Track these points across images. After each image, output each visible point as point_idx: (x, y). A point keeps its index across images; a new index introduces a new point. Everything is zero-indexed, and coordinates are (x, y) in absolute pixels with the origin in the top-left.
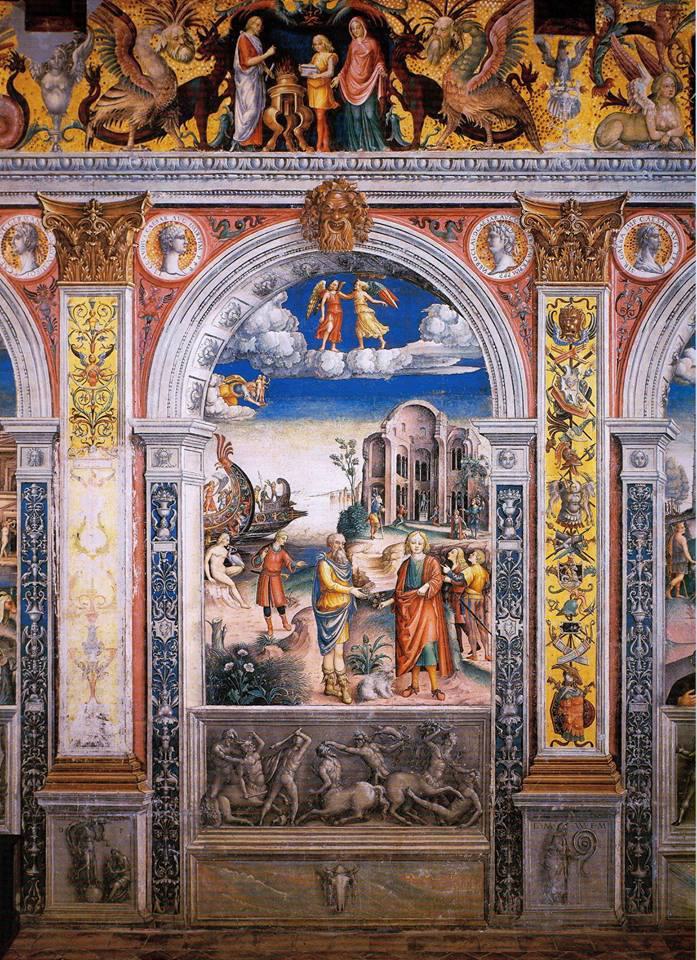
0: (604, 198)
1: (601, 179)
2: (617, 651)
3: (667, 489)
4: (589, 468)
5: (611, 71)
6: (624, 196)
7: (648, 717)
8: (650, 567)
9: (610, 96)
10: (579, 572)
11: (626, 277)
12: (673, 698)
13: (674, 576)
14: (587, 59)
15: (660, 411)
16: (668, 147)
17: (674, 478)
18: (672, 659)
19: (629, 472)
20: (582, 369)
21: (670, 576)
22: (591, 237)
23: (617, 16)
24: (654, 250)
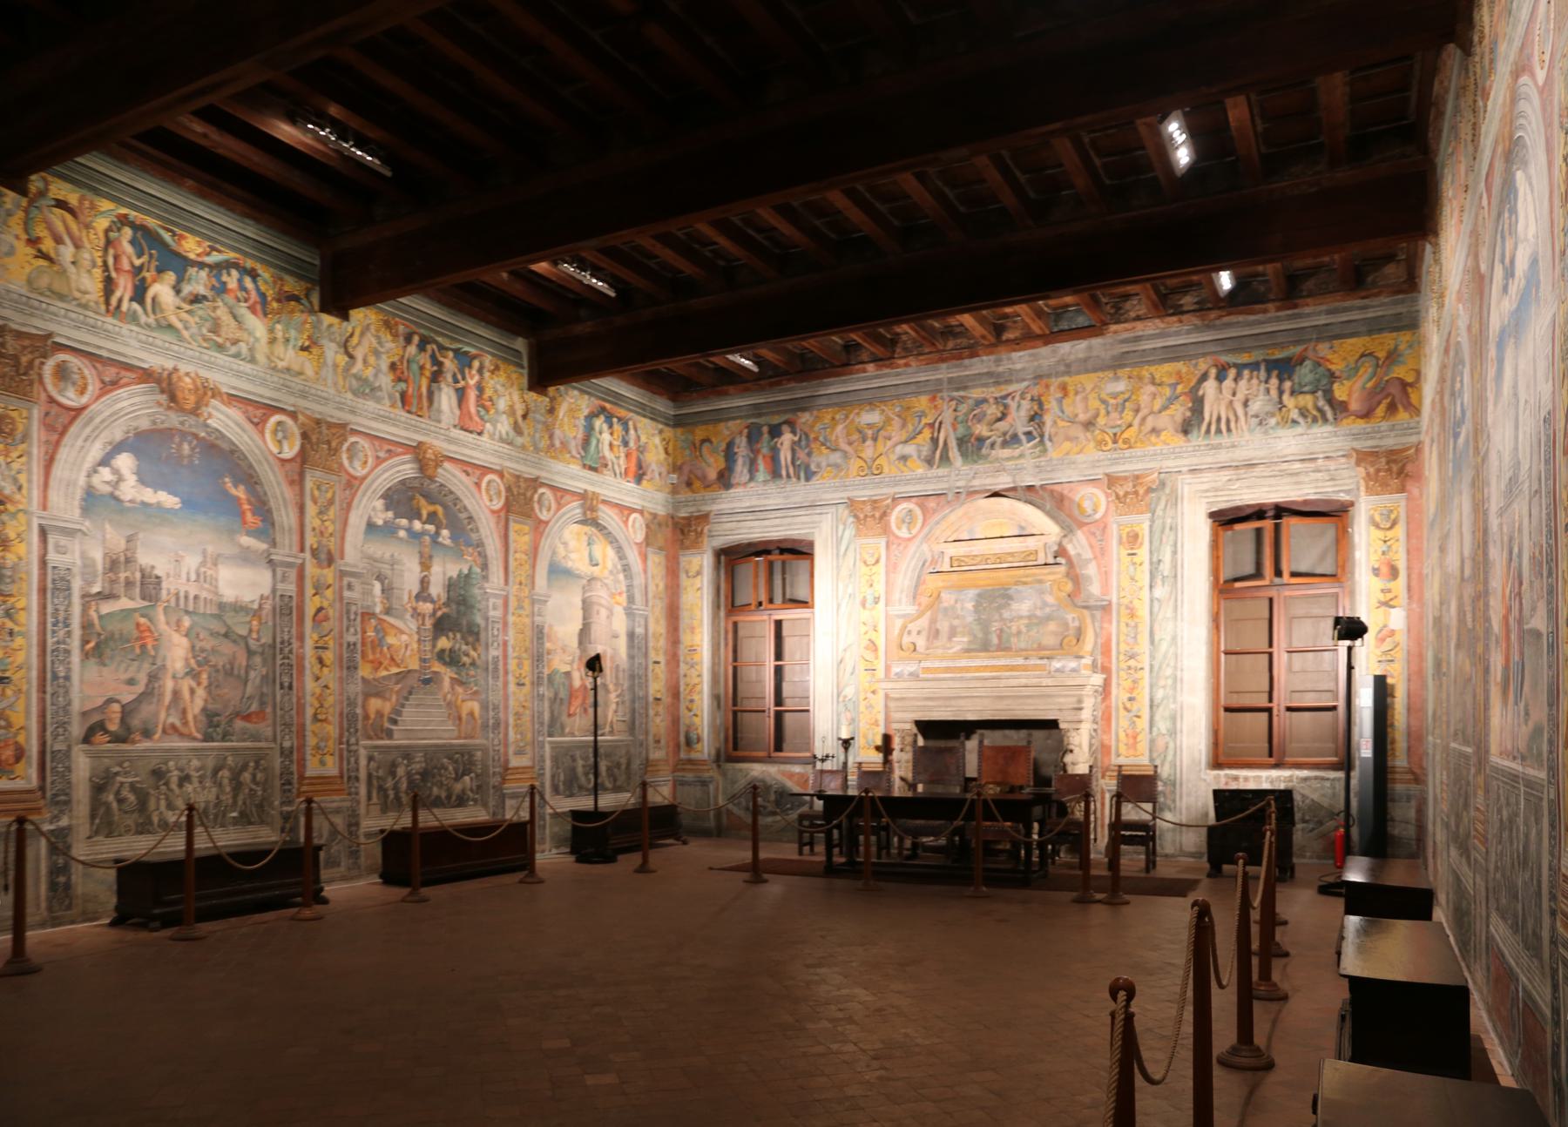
0: (34, 331)
1: (32, 315)
2: (42, 701)
3: (83, 574)
4: (21, 549)
5: (40, 231)
6: (50, 335)
7: (67, 754)
8: (69, 634)
9: (40, 251)
10: (11, 633)
11: (52, 400)
12: (87, 739)
13: (88, 642)
14: (21, 214)
15: (77, 512)
16: (85, 306)
17: (88, 564)
18: (89, 706)
19: (52, 557)
20: (15, 466)
21: (85, 642)
22: (24, 360)
23: (47, 190)
24: (74, 384)
